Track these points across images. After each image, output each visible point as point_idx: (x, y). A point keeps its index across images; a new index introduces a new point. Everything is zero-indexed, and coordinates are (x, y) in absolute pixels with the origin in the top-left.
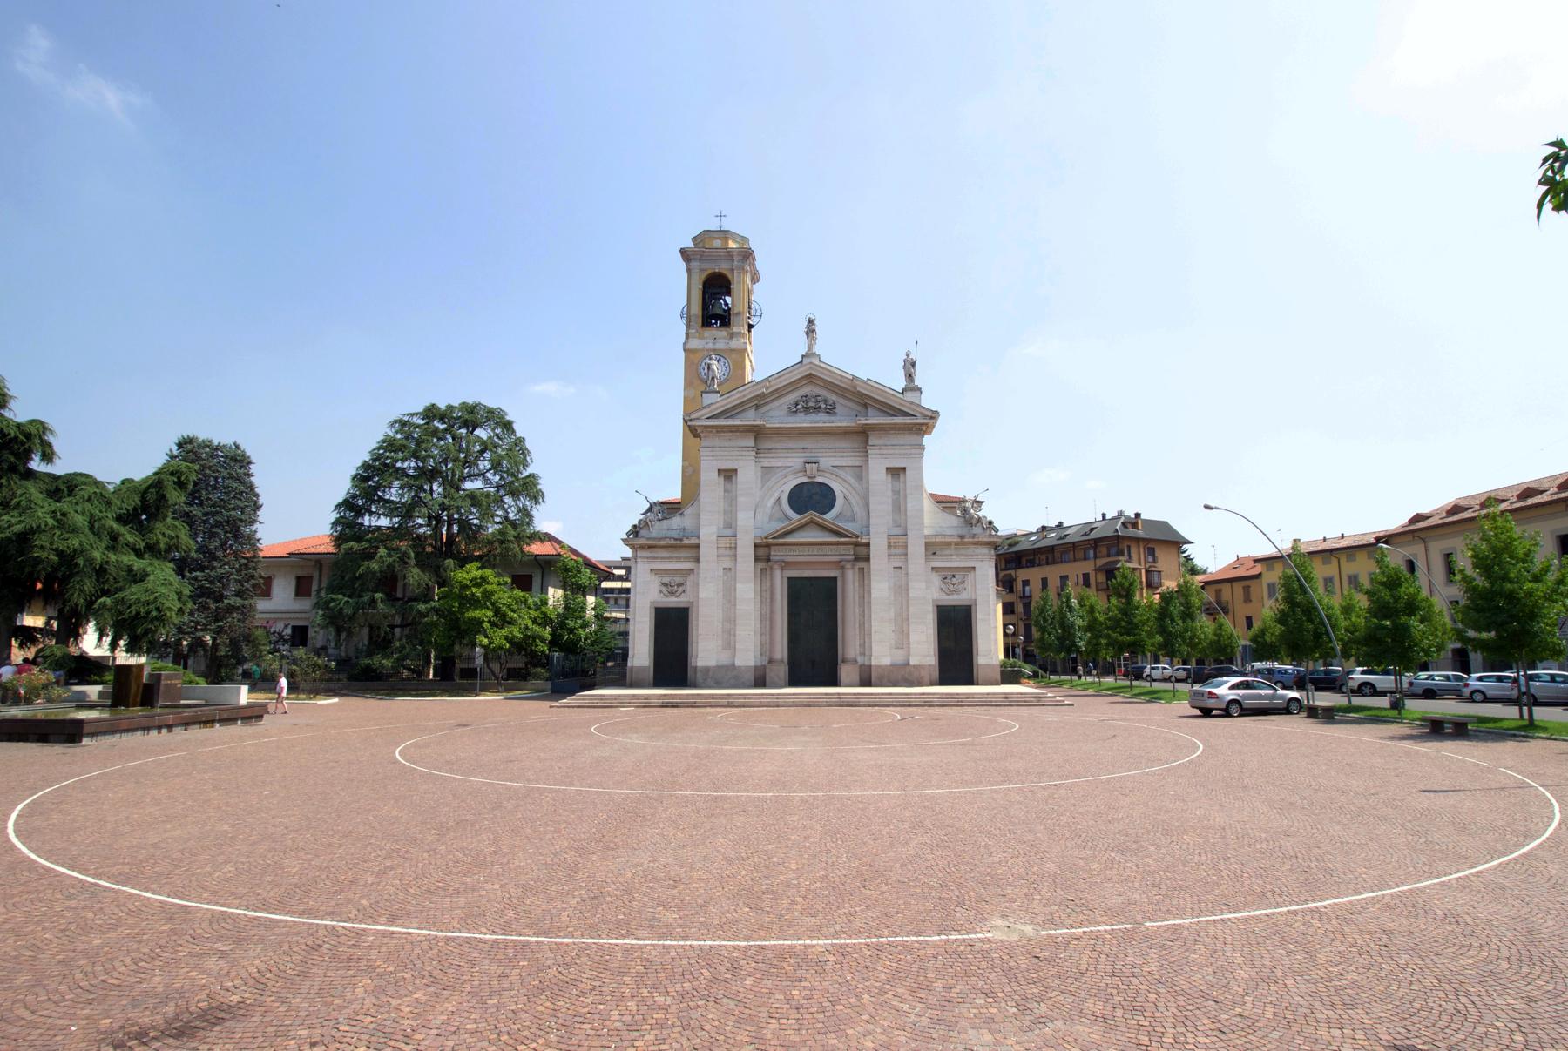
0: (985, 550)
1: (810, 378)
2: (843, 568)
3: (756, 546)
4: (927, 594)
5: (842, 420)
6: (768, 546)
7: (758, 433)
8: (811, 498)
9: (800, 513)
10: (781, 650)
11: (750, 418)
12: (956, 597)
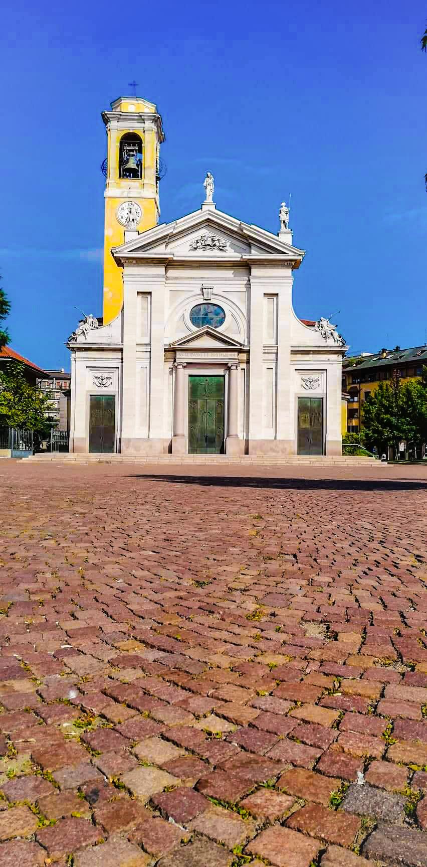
1: (208, 220)
2: (229, 369)
3: (165, 350)
4: (293, 388)
5: (232, 254)
6: (174, 351)
7: (168, 263)
8: (206, 316)
9: (198, 327)
10: (184, 428)
11: (160, 251)
12: (311, 391)
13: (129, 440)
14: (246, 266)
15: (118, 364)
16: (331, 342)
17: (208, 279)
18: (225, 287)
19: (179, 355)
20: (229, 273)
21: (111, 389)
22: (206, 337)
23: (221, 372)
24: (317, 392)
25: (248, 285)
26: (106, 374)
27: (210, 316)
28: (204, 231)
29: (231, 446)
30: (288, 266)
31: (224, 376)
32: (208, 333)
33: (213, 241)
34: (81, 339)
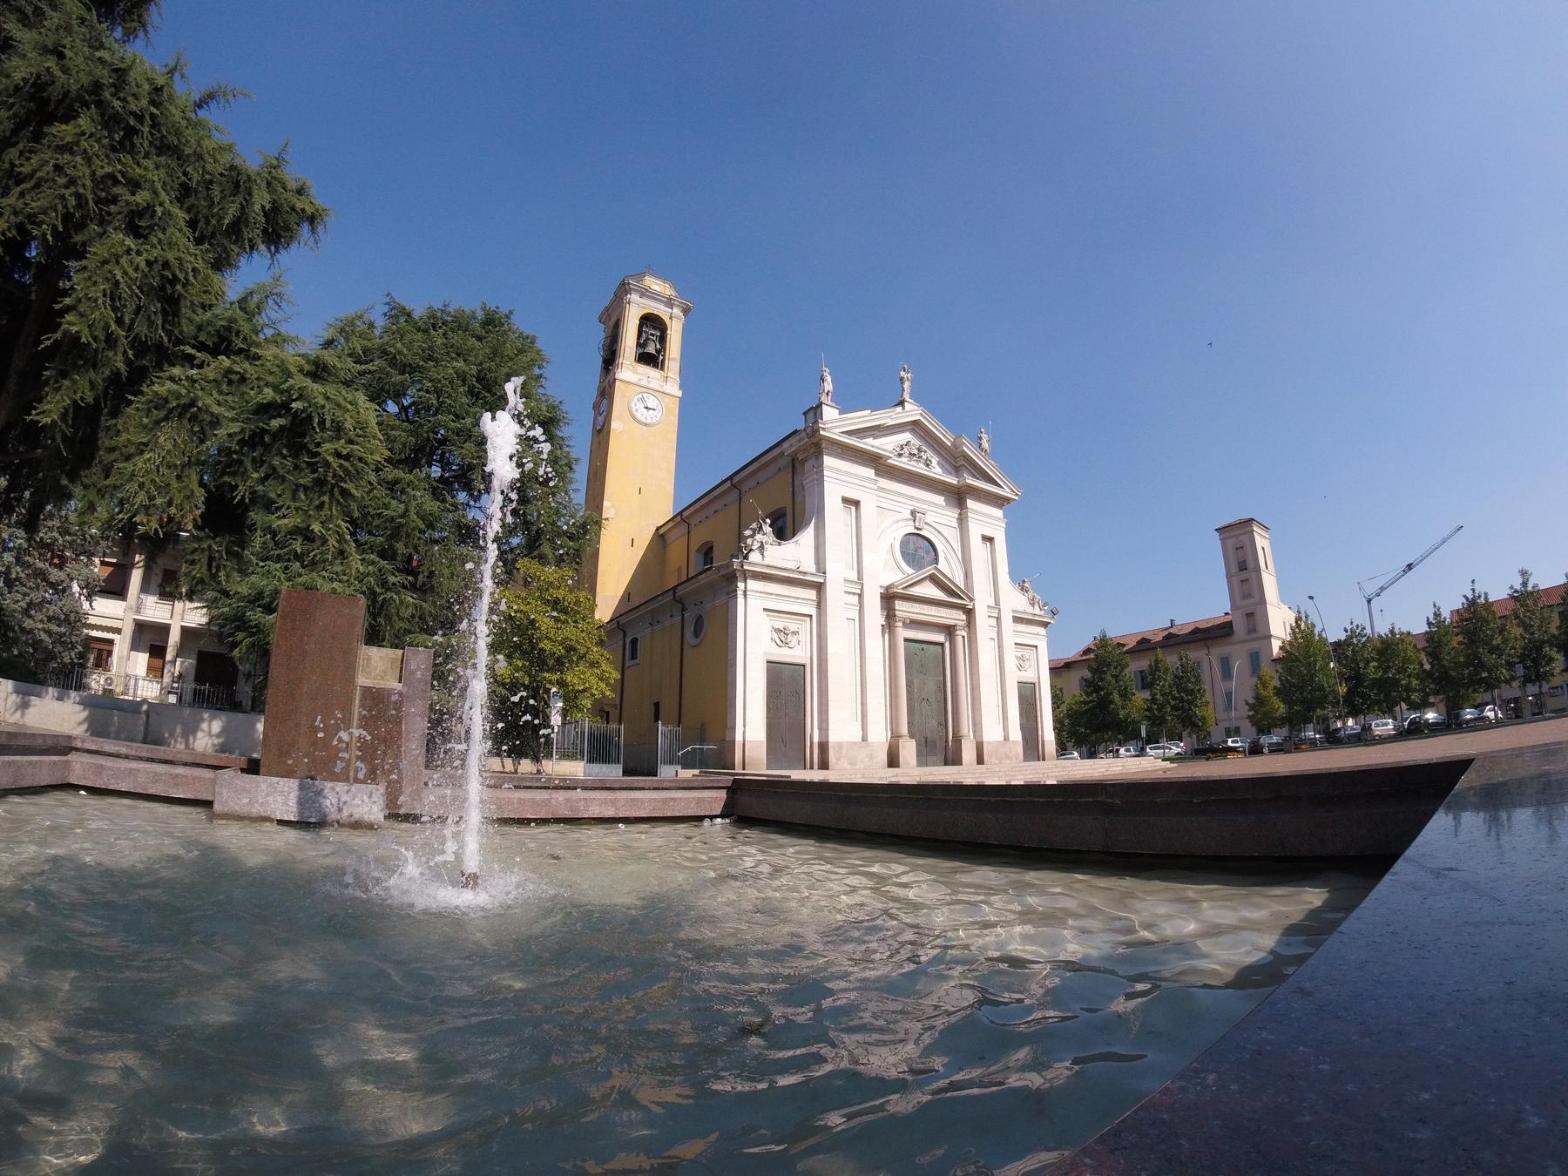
0: (1042, 630)
1: (916, 423)
5: (937, 471)
13: (840, 745)
14: (958, 497)
15: (812, 611)
16: (1037, 611)
17: (918, 500)
18: (938, 516)
19: (900, 605)
20: (940, 500)
21: (799, 652)
22: (928, 583)
23: (940, 638)
24: (1029, 675)
25: (962, 520)
26: (792, 626)
27: (921, 552)
28: (906, 436)
29: (968, 753)
30: (1000, 506)
31: (942, 645)
32: (933, 579)
33: (919, 450)
34: (754, 557)
